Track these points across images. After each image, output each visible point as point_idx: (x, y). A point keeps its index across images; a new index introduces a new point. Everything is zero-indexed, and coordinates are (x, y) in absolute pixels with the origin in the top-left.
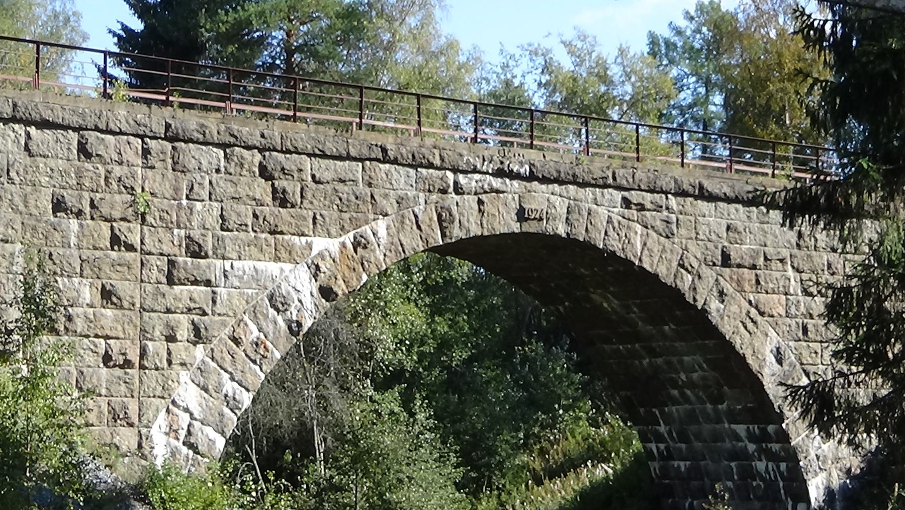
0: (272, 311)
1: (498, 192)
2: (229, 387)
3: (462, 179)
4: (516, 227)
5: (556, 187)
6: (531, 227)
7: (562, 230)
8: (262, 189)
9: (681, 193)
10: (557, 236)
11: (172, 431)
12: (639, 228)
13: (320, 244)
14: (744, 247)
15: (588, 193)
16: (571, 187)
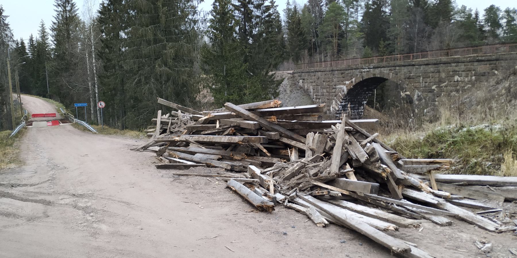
0: (342, 92)
1: (369, 71)
2: (338, 102)
3: (364, 70)
4: (372, 76)
5: (378, 69)
6: (374, 76)
7: (379, 76)
8: (341, 76)
9: (398, 66)
10: (378, 77)
11: (333, 108)
12: (391, 74)
13: (347, 82)
14: (411, 75)
15: (382, 69)
16: (380, 69)
